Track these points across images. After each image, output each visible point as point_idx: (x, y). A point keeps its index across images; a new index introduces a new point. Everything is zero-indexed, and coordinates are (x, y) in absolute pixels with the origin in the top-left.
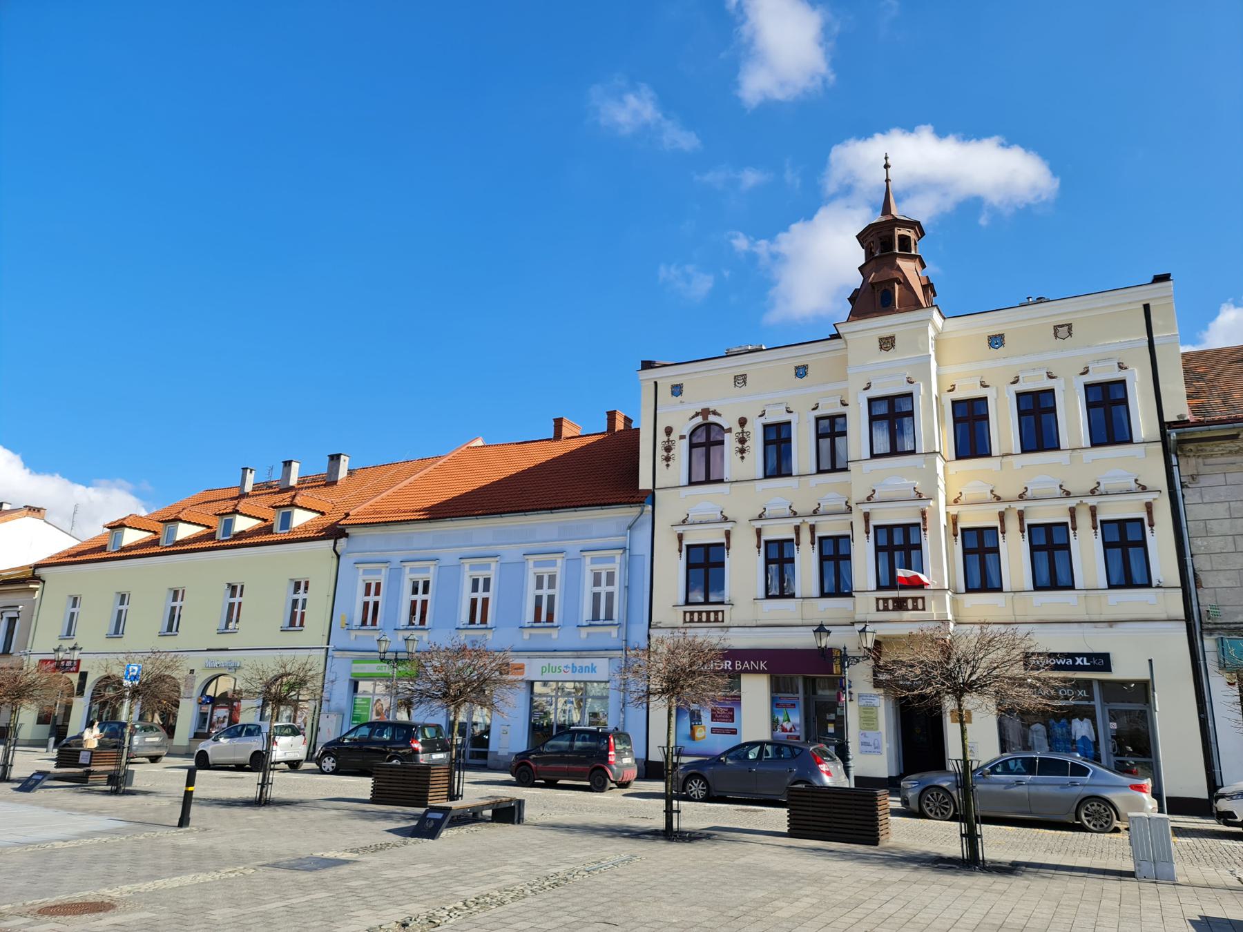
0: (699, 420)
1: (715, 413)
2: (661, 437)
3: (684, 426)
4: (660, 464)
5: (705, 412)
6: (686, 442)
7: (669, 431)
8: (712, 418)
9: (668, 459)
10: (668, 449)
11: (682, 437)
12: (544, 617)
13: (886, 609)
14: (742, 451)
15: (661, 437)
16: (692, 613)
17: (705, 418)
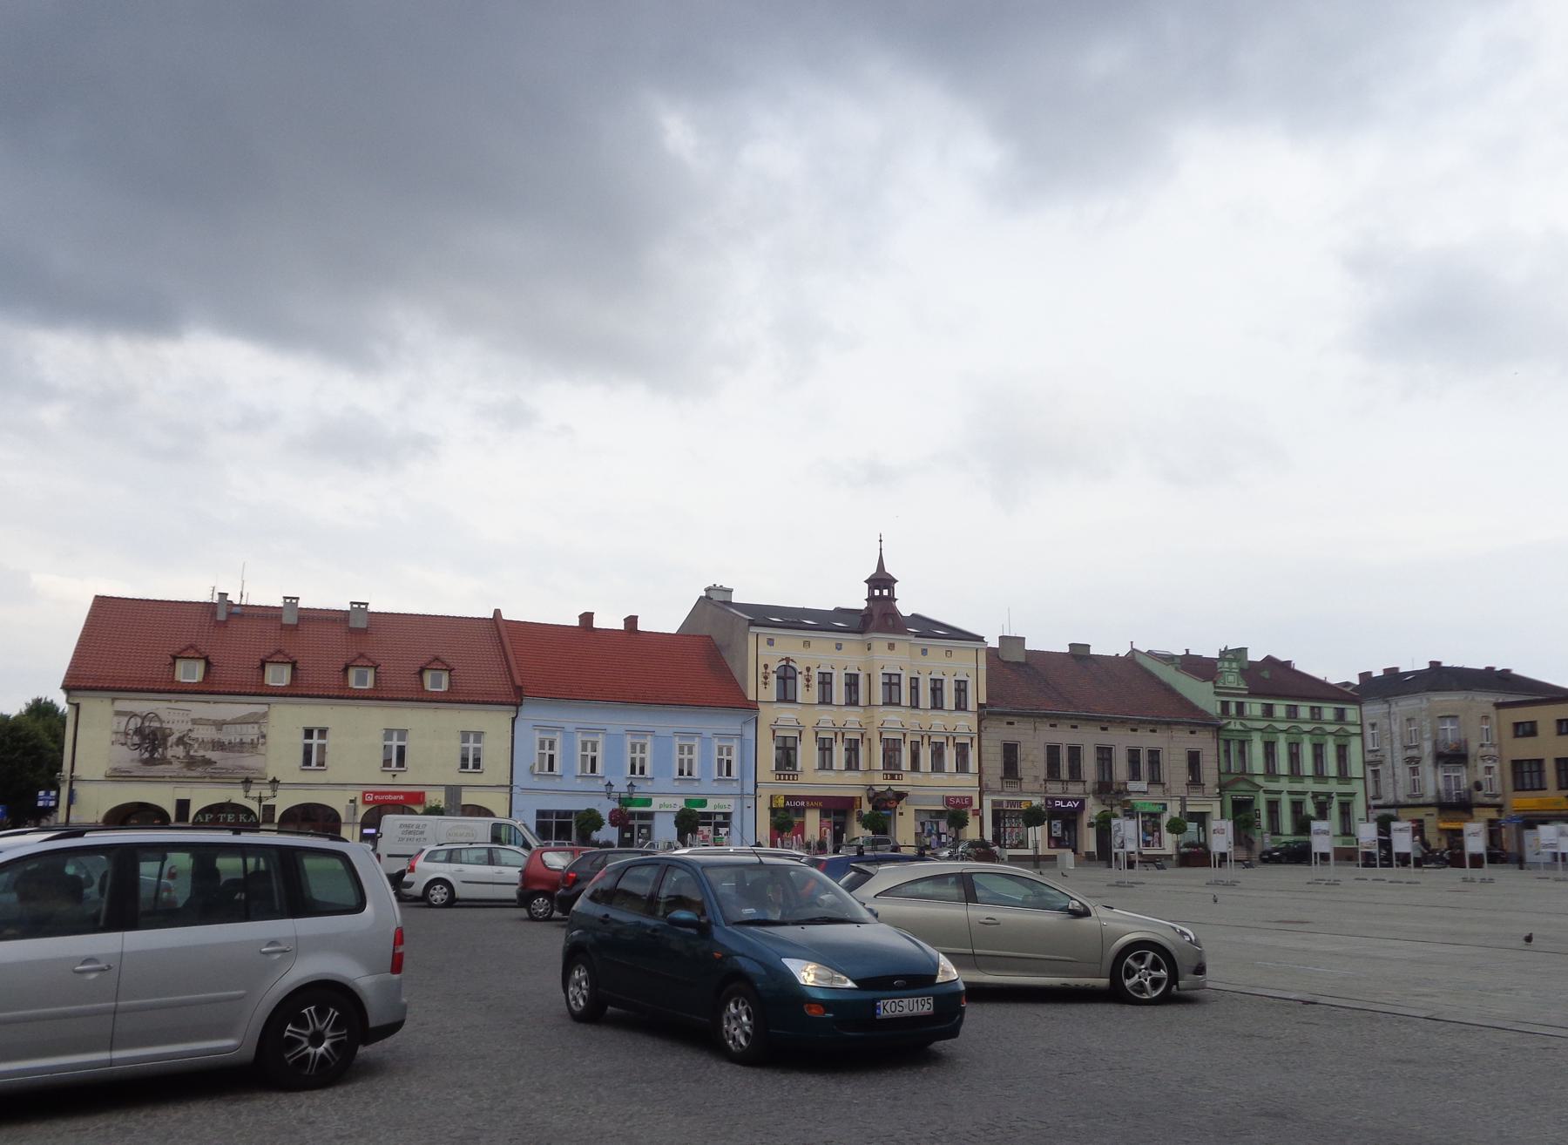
0: (784, 663)
1: (792, 660)
2: (762, 669)
3: (774, 666)
4: (761, 686)
5: (787, 659)
6: (775, 675)
7: (766, 666)
8: (791, 664)
9: (766, 684)
10: (766, 678)
11: (774, 672)
12: (685, 773)
13: (887, 779)
14: (808, 686)
15: (762, 669)
16: (780, 775)
17: (788, 662)
